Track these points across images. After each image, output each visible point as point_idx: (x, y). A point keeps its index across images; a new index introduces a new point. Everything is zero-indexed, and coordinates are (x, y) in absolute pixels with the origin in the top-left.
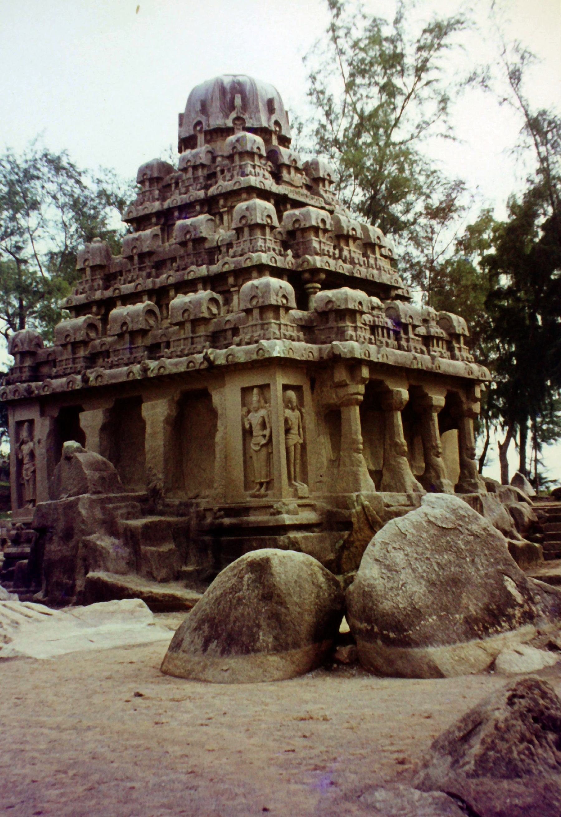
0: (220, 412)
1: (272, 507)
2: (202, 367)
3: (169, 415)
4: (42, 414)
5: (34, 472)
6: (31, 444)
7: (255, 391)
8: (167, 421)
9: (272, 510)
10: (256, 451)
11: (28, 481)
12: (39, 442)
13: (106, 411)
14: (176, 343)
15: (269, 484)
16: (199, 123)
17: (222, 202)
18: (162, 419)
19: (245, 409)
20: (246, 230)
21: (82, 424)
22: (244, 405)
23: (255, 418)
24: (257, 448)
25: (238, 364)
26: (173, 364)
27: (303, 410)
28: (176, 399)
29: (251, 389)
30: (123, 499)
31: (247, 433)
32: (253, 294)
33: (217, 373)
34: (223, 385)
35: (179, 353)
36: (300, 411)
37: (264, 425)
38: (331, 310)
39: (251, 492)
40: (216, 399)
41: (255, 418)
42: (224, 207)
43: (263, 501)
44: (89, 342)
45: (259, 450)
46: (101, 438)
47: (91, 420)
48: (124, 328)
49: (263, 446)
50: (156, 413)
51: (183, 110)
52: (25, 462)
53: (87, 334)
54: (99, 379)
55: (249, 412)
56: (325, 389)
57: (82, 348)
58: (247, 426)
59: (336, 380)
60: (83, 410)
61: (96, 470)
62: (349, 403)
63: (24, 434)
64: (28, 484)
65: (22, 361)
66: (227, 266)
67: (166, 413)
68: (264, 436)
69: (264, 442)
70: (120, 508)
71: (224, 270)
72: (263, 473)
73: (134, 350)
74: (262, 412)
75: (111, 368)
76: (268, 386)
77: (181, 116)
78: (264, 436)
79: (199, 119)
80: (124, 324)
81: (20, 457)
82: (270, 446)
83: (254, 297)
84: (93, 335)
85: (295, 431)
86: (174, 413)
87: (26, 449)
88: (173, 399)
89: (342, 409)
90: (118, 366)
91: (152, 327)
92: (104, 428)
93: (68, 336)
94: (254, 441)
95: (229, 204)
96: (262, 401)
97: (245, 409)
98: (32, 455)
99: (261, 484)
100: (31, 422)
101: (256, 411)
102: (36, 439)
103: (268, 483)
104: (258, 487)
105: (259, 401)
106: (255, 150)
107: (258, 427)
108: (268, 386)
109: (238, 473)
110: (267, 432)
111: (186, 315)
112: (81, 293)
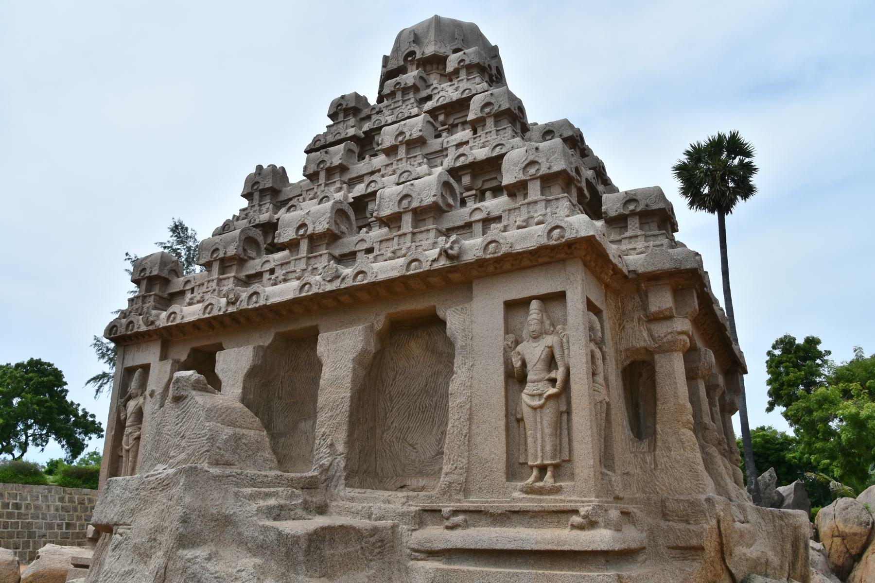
0: (459, 343)
1: (576, 512)
2: (436, 266)
3: (364, 351)
4: (163, 357)
5: (138, 438)
6: (141, 400)
7: (534, 304)
8: (359, 361)
9: (576, 519)
10: (534, 409)
11: (128, 451)
12: (152, 394)
13: (257, 349)
14: (384, 245)
15: (560, 468)
16: (413, 53)
17: (441, 118)
18: (352, 356)
19: (511, 337)
20: (490, 122)
21: (218, 369)
22: (507, 331)
23: (533, 352)
24: (536, 403)
25: (508, 256)
26: (384, 268)
27: (604, 349)
28: (378, 326)
29: (523, 304)
30: (277, 482)
31: (516, 377)
32: (531, 158)
33: (460, 278)
34: (470, 298)
35: (390, 255)
36: (601, 349)
37: (551, 362)
38: (633, 214)
39: (520, 484)
40: (454, 319)
41: (533, 352)
42: (443, 124)
43: (549, 502)
44: (246, 261)
45: (541, 407)
46: (244, 388)
47: (234, 362)
48: (301, 232)
49: (550, 397)
50: (340, 351)
51: (388, 54)
52: (128, 424)
53: (245, 250)
54: (254, 298)
55: (517, 343)
56: (628, 326)
57: (234, 268)
58: (517, 364)
59: (653, 308)
60: (222, 349)
61: (232, 424)
62: (667, 349)
63: (133, 385)
64: (127, 456)
65: (148, 290)
66: (462, 159)
67: (359, 347)
68: (553, 381)
69: (552, 391)
70: (268, 495)
71: (458, 164)
72: (548, 448)
73: (312, 261)
74: (549, 340)
75: (275, 284)
76: (561, 296)
77: (386, 58)
78: (553, 381)
79: (412, 49)
80: (303, 225)
81: (122, 418)
82: (563, 399)
83: (533, 163)
84: (252, 253)
85: (600, 379)
86: (372, 348)
87: (132, 405)
88: (372, 326)
89: (657, 357)
90: (285, 280)
91: (343, 233)
92: (251, 374)
93: (217, 250)
94: (529, 388)
95: (451, 121)
96: (548, 322)
97: (511, 337)
98: (139, 414)
99: (543, 469)
100: (146, 368)
101: (536, 337)
102: (147, 393)
103: (556, 467)
104: (535, 473)
105: (542, 322)
106: (486, 65)
107: (540, 366)
108: (561, 296)
109: (493, 447)
110: (559, 374)
111: (405, 203)
112: (243, 219)
